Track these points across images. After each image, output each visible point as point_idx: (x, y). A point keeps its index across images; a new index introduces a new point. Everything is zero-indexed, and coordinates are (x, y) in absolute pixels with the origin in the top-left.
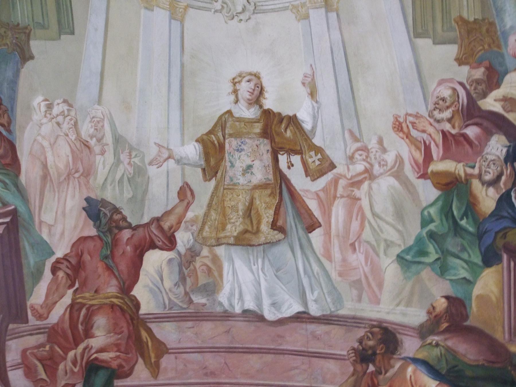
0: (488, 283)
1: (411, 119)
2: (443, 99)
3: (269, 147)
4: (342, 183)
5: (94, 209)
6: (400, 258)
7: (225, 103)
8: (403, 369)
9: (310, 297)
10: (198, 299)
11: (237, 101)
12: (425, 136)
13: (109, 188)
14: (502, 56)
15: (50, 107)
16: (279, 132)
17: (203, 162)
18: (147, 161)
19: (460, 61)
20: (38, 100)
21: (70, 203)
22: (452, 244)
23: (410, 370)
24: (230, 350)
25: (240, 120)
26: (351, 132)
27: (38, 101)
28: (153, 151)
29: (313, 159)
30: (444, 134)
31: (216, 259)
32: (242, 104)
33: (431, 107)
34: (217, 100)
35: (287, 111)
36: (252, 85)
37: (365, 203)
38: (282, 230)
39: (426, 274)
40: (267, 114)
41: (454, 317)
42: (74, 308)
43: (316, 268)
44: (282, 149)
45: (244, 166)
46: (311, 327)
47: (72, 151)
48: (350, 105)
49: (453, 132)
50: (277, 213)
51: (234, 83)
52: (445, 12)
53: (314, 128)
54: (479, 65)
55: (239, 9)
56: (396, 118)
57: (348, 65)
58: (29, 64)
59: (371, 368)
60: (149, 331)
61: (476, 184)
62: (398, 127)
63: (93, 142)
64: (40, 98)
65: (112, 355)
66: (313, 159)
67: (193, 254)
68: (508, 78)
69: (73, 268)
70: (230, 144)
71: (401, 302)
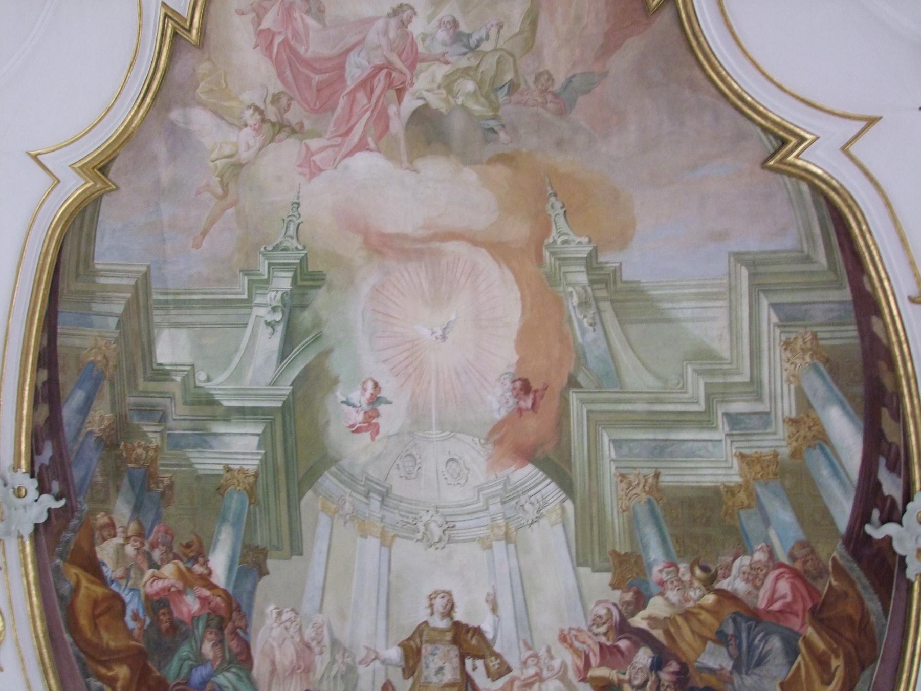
1: (573, 632)
2: (600, 617)
3: (457, 652)
4: (517, 684)
7: (423, 615)
11: (432, 614)
12: (585, 647)
13: (325, 683)
14: (648, 583)
15: (280, 614)
16: (466, 640)
17: (403, 663)
18: (358, 660)
19: (614, 586)
20: (271, 609)
25: (434, 629)
26: (526, 644)
27: (271, 609)
28: (362, 653)
29: (494, 663)
30: (601, 646)
32: (437, 617)
33: (590, 623)
34: (415, 613)
35: (473, 623)
36: (445, 600)
40: (457, 625)
44: (468, 654)
45: (437, 666)
47: (297, 652)
48: (524, 620)
49: (609, 644)
51: (431, 598)
52: (602, 546)
53: (495, 637)
54: (628, 590)
55: (437, 539)
56: (562, 631)
57: (523, 586)
58: (265, 579)
62: (563, 639)
63: (314, 644)
64: (272, 607)
68: (652, 600)
70: (426, 649)
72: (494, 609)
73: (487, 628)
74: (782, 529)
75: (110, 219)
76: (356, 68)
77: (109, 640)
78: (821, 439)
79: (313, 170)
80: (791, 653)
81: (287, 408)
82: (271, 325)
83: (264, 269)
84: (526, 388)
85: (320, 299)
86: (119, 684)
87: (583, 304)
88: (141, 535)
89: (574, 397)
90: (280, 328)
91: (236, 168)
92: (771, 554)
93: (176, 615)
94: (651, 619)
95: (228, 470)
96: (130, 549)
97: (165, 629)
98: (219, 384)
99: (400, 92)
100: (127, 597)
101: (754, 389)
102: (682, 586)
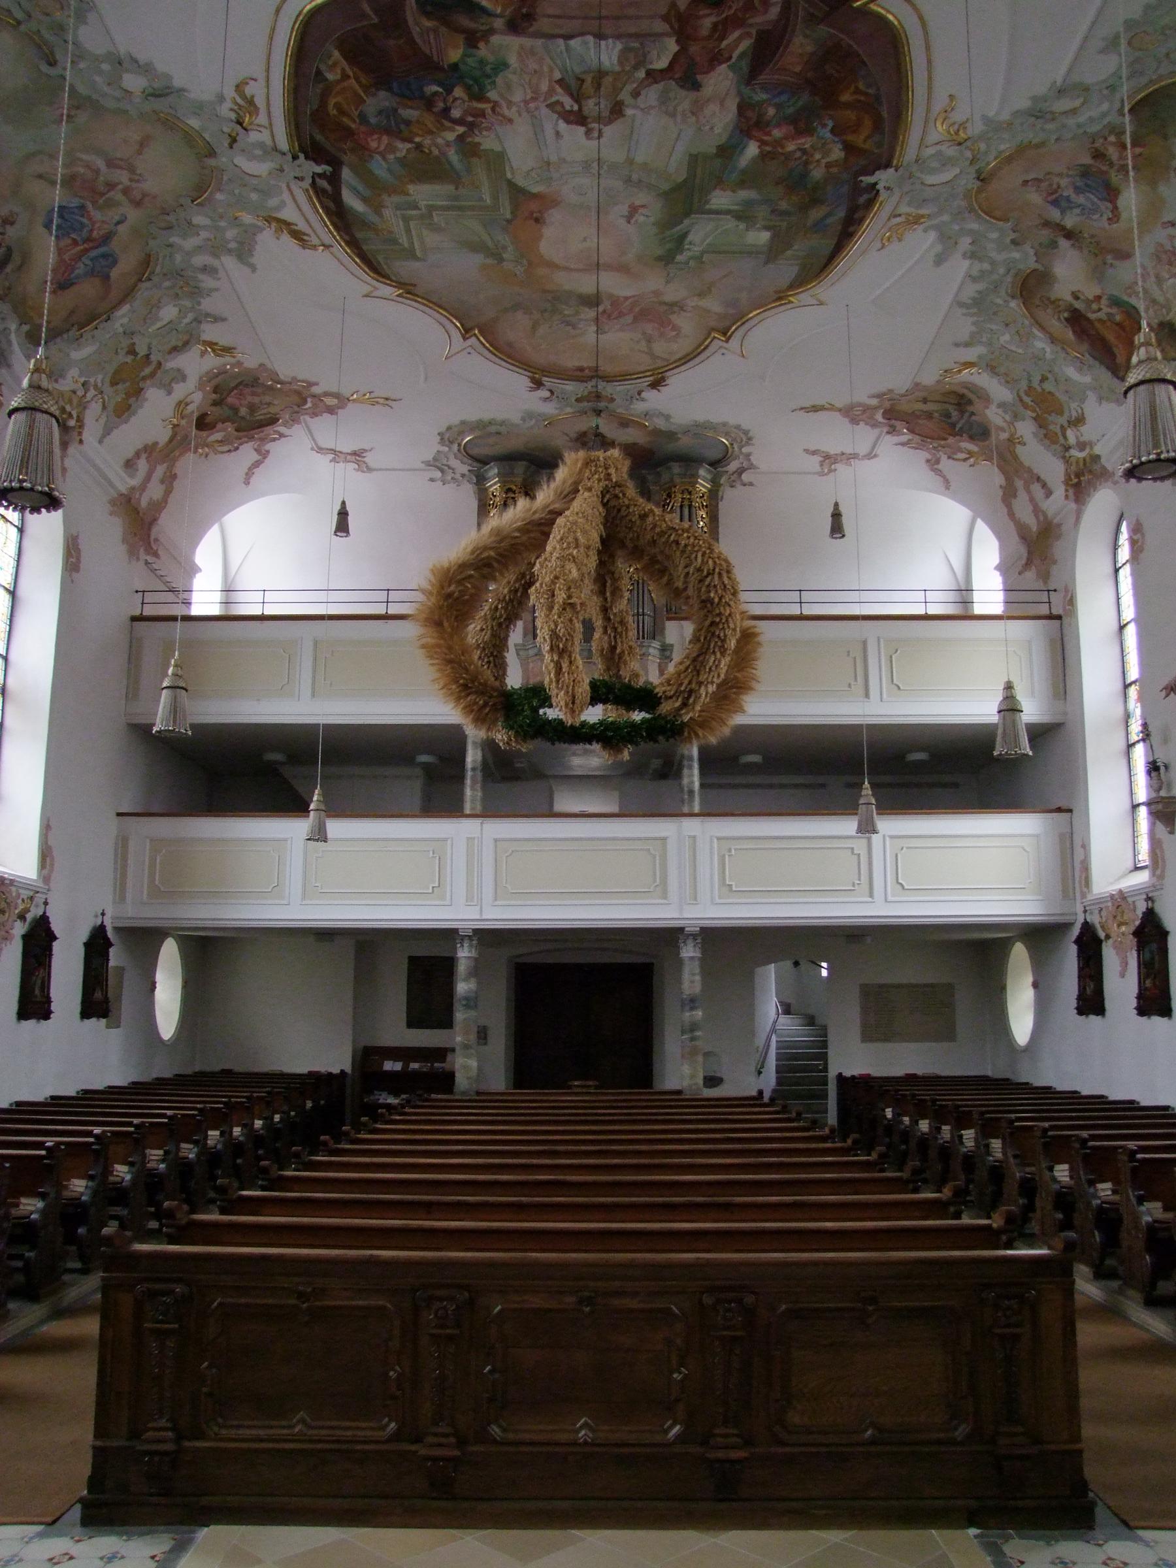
0: (454, 55)
5: (696, 86)
6: (506, 65)
8: (503, 10)
9: (563, 48)
10: (636, 45)
15: (712, 128)
16: (578, 118)
21: (711, 89)
22: (477, 73)
23: (499, 11)
24: (618, 18)
28: (653, 112)
31: (620, 63)
35: (574, 127)
37: (529, 91)
38: (578, 79)
39: (491, 58)
40: (583, 124)
41: (472, 40)
42: (722, 38)
43: (558, 62)
46: (562, 32)
50: (581, 87)
54: (469, 143)
59: (524, 11)
60: (672, 27)
61: (466, 98)
62: (510, 121)
65: (701, 13)
66: (558, 108)
67: (636, 67)
69: (716, 59)
71: (507, 46)
72: (557, 133)
73: (562, 125)
74: (379, 168)
75: (784, 282)
76: (629, 319)
77: (851, 115)
78: (365, 200)
79: (657, 293)
80: (363, 118)
81: (687, 214)
82: (690, 243)
83: (692, 263)
84: (537, 220)
85: (659, 252)
86: (852, 89)
87: (504, 248)
88: (806, 163)
89: (509, 216)
90: (686, 242)
91: (701, 295)
92: (384, 158)
93: (791, 128)
94: (453, 130)
95: (734, 191)
96: (818, 156)
97: (801, 124)
98: (730, 223)
99: (604, 311)
100: (828, 135)
101: (407, 220)
102: (437, 146)
